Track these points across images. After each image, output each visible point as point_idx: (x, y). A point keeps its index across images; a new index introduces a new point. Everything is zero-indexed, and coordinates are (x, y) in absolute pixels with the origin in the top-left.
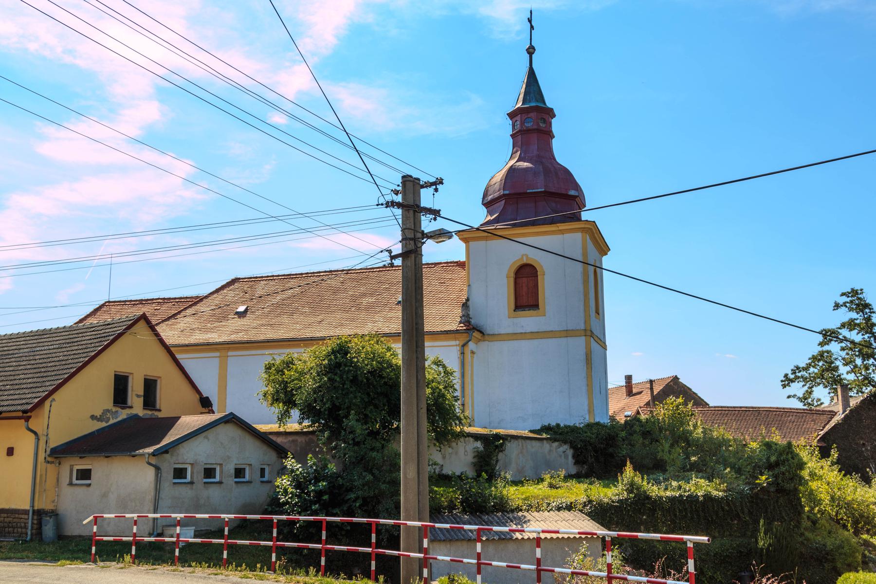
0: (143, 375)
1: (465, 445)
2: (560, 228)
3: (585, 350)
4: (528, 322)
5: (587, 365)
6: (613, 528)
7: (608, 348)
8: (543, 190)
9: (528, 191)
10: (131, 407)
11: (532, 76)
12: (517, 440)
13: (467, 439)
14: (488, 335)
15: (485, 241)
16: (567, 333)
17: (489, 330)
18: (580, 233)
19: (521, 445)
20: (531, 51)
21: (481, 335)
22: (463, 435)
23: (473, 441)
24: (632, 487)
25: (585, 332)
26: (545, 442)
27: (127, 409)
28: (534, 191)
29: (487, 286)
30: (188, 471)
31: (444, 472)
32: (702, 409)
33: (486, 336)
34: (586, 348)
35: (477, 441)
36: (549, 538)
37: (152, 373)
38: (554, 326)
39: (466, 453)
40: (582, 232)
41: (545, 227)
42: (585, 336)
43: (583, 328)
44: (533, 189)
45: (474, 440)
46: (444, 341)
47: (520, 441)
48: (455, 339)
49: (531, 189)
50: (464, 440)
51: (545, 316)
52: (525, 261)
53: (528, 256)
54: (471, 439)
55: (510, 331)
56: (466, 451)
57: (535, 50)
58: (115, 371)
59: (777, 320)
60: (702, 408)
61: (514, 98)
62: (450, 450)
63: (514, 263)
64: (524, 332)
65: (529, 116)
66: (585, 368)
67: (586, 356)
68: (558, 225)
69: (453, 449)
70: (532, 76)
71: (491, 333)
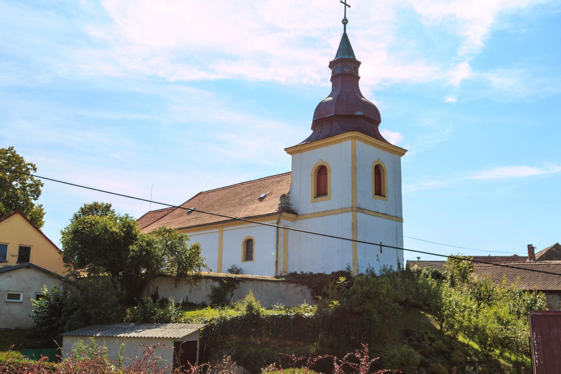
0: (18, 245)
1: (206, 284)
2: (338, 138)
3: (351, 221)
4: (323, 204)
5: (352, 232)
6: (231, 336)
7: (404, 220)
8: (334, 114)
9: (326, 116)
10: (7, 262)
11: (345, 39)
12: (252, 281)
13: (208, 280)
14: (300, 215)
15: (300, 154)
16: (343, 211)
17: (301, 212)
18: (351, 140)
19: (256, 285)
20: (345, 22)
21: (295, 215)
22: (198, 277)
23: (213, 282)
24: (250, 308)
25: (352, 209)
26: (281, 283)
27: (3, 263)
28: (330, 115)
29: (300, 183)
30: (21, 296)
31: (189, 301)
32: (519, 264)
33: (299, 216)
34: (352, 220)
35: (216, 282)
36: (136, 337)
37: (25, 243)
38: (335, 207)
39: (207, 289)
40: (351, 139)
41: (329, 139)
42: (352, 211)
43: (351, 206)
44: (329, 114)
45: (213, 281)
46: (269, 221)
47: (255, 282)
48: (272, 219)
49: (328, 115)
50: (206, 281)
51: (330, 199)
52: (320, 164)
53: (322, 160)
54: (211, 280)
55: (312, 211)
56: (206, 288)
57: (348, 21)
58: (19, 244)
59: (38, 176)
60: (520, 263)
61: (332, 54)
62: (195, 287)
63: (315, 165)
64: (319, 211)
65: (337, 66)
66: (352, 234)
67: (352, 226)
68: (336, 136)
69: (197, 286)
70: (345, 39)
71: (302, 214)
